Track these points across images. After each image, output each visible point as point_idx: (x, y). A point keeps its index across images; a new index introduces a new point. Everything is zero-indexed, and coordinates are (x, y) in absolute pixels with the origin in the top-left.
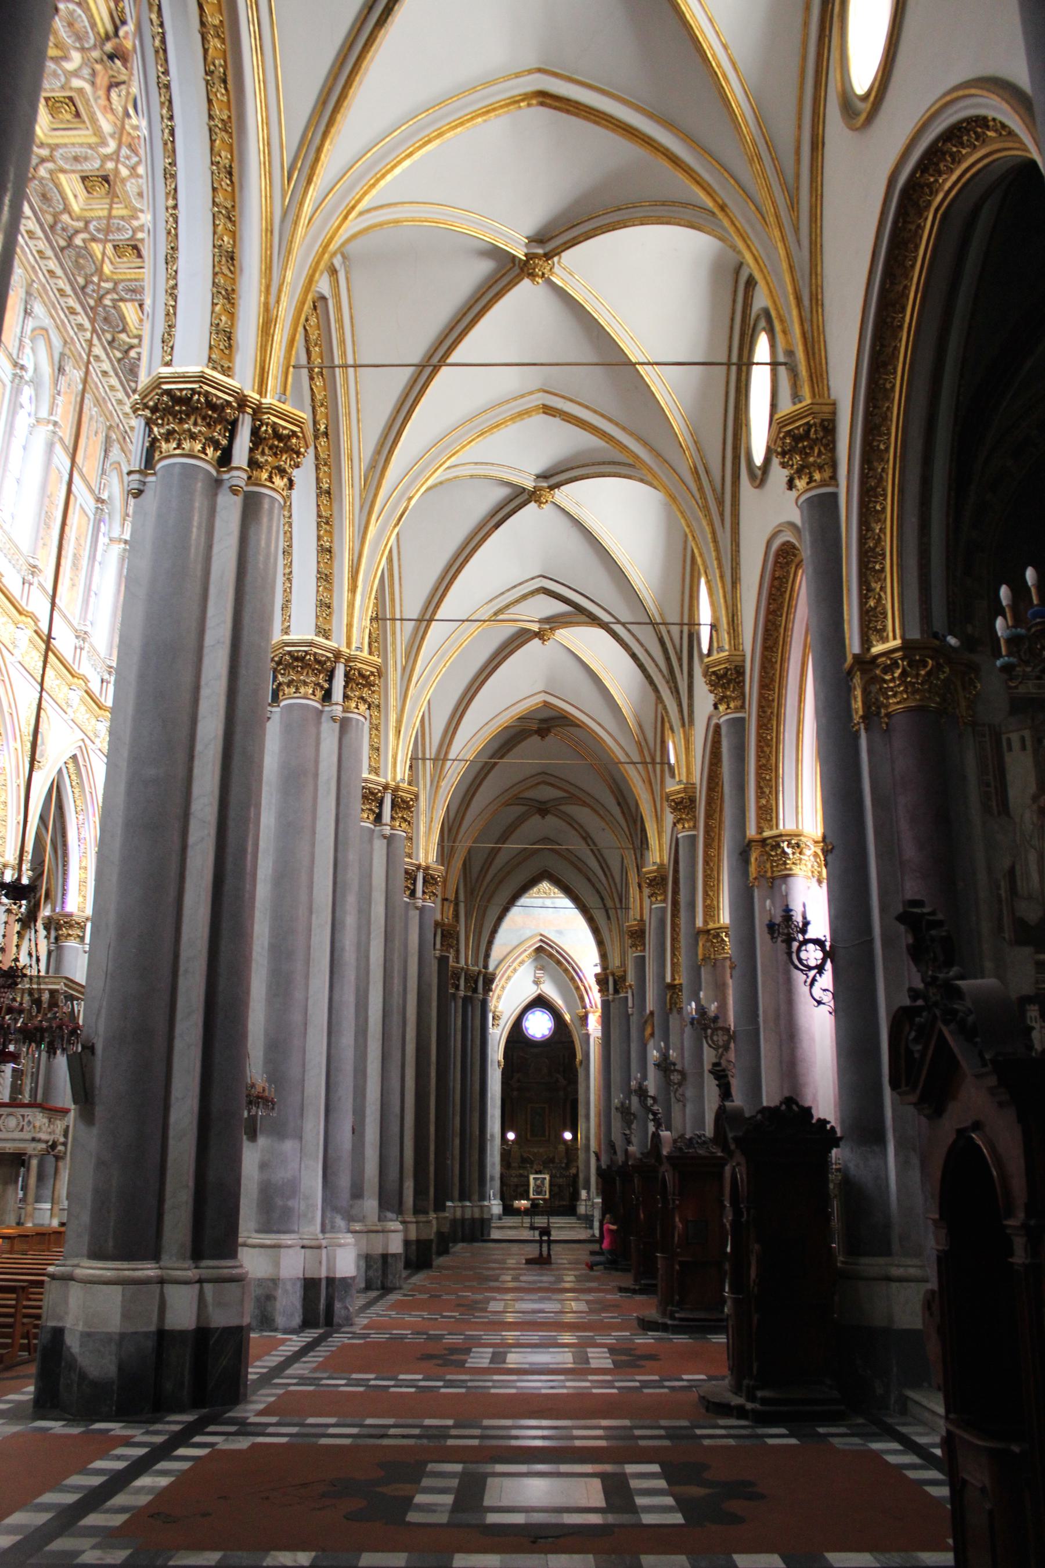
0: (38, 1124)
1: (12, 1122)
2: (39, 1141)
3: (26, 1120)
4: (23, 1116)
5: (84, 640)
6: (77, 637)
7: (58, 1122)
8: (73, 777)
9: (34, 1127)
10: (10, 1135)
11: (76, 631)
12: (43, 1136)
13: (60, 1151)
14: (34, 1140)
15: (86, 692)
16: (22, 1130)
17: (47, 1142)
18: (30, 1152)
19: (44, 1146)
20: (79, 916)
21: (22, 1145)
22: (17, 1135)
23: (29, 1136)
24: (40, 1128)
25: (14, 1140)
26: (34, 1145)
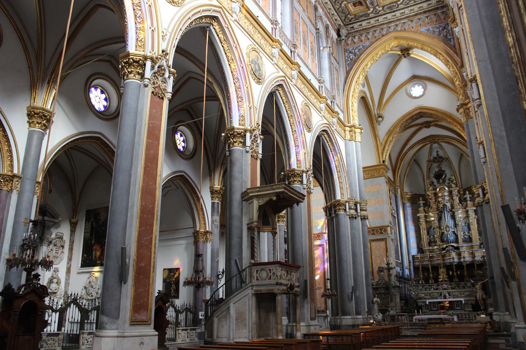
0: (279, 274)
1: (264, 274)
2: (281, 284)
3: (272, 272)
4: (270, 270)
5: (276, 25)
6: (272, 24)
7: (293, 274)
8: (284, 98)
9: (277, 276)
10: (264, 282)
11: (271, 21)
12: (283, 282)
13: (296, 291)
14: (277, 284)
15: (281, 50)
16: (270, 279)
17: (286, 285)
18: (276, 291)
19: (285, 288)
20: (298, 170)
21: (271, 288)
22: (268, 282)
23: (274, 282)
24: (281, 276)
25: (266, 285)
26: (277, 287)
